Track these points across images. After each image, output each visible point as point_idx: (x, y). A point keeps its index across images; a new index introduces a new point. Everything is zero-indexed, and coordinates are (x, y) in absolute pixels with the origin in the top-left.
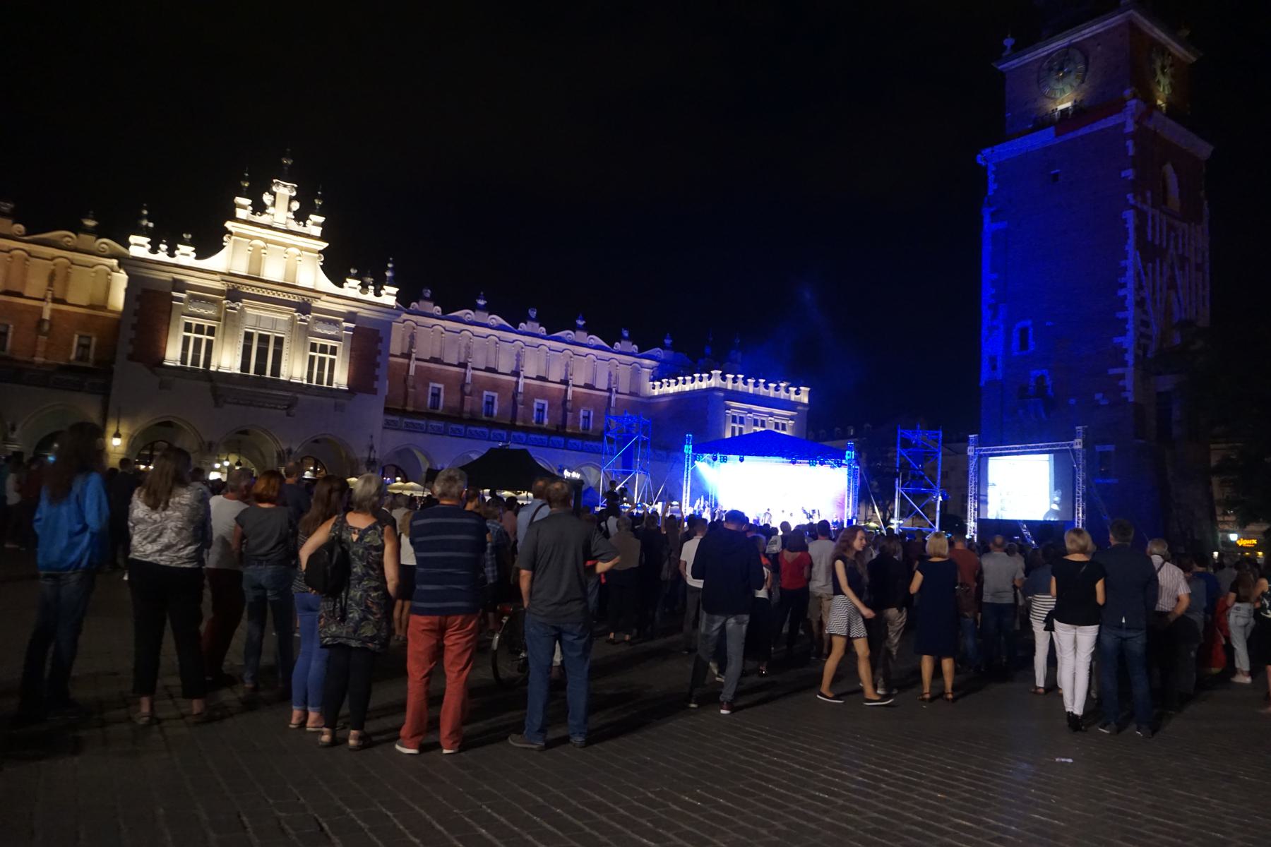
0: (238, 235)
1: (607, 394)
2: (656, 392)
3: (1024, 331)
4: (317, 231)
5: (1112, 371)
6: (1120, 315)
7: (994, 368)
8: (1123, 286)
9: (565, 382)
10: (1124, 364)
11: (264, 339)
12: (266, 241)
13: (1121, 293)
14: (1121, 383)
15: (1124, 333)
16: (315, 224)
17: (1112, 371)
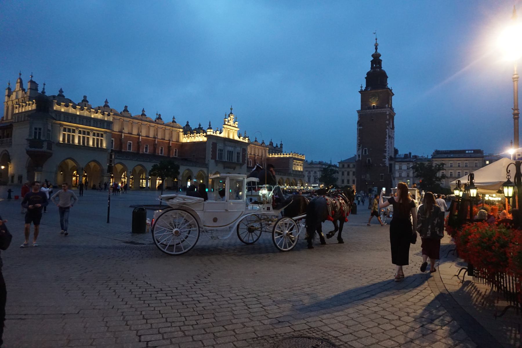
0: (226, 128)
1: (168, 142)
2: (270, 156)
3: (365, 150)
4: (237, 126)
5: (383, 160)
6: (385, 149)
7: (359, 157)
8: (386, 144)
9: (121, 132)
10: (386, 159)
11: (230, 151)
12: (230, 129)
13: (386, 145)
14: (385, 162)
15: (386, 153)
16: (237, 124)
17: (383, 160)
